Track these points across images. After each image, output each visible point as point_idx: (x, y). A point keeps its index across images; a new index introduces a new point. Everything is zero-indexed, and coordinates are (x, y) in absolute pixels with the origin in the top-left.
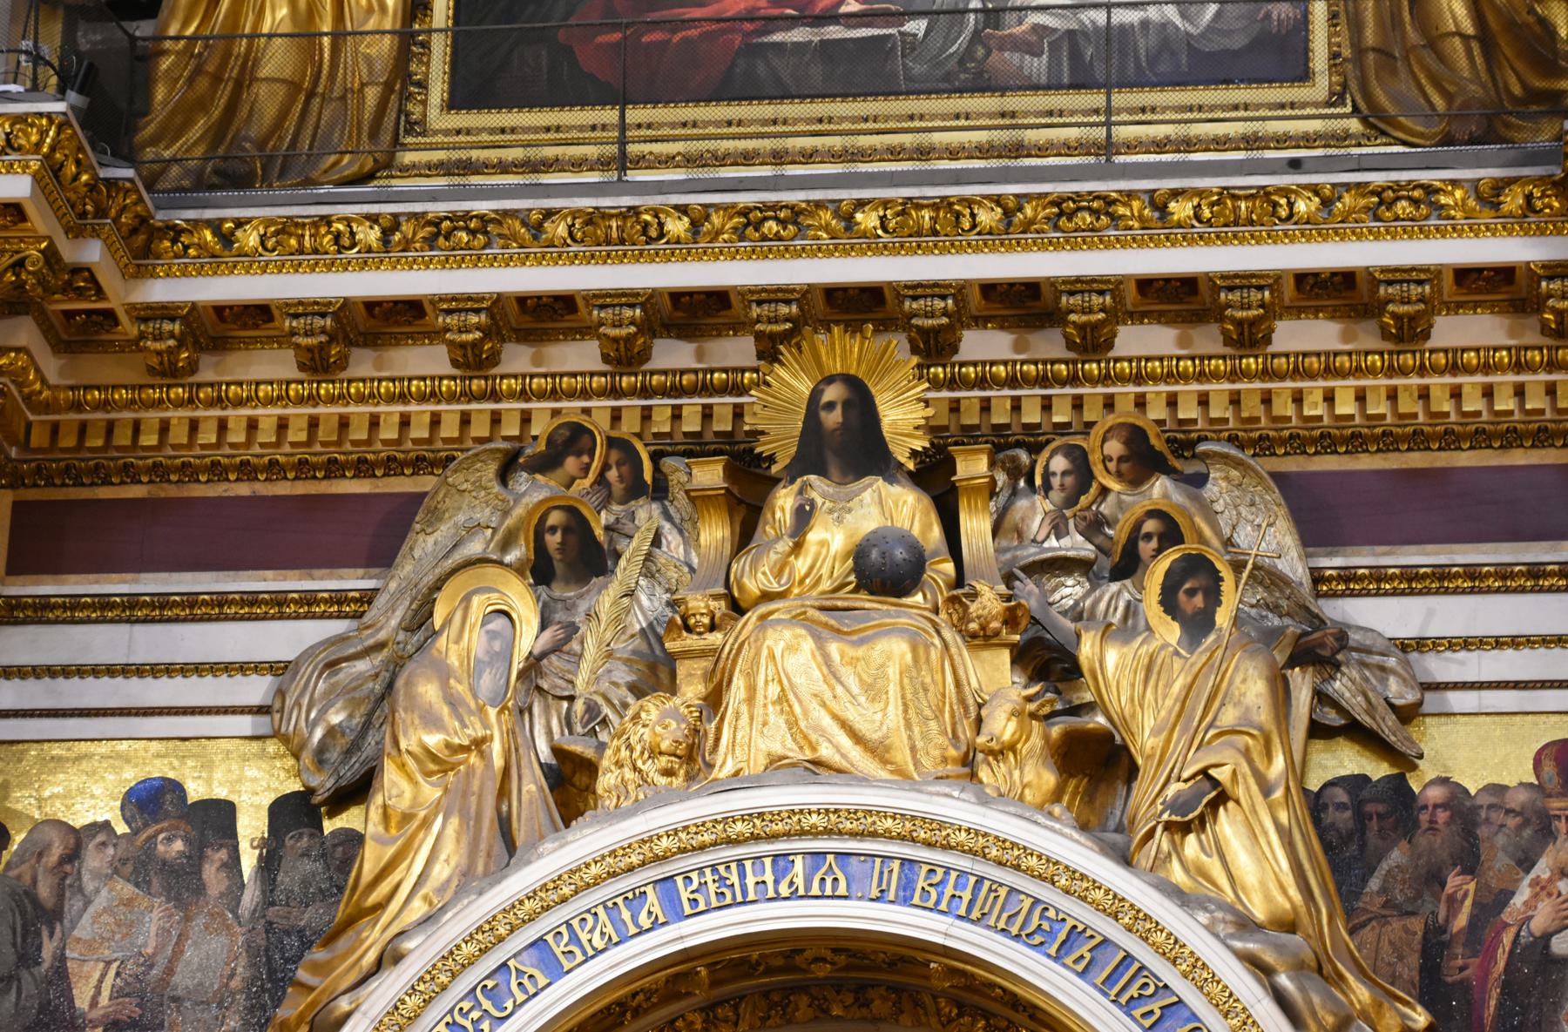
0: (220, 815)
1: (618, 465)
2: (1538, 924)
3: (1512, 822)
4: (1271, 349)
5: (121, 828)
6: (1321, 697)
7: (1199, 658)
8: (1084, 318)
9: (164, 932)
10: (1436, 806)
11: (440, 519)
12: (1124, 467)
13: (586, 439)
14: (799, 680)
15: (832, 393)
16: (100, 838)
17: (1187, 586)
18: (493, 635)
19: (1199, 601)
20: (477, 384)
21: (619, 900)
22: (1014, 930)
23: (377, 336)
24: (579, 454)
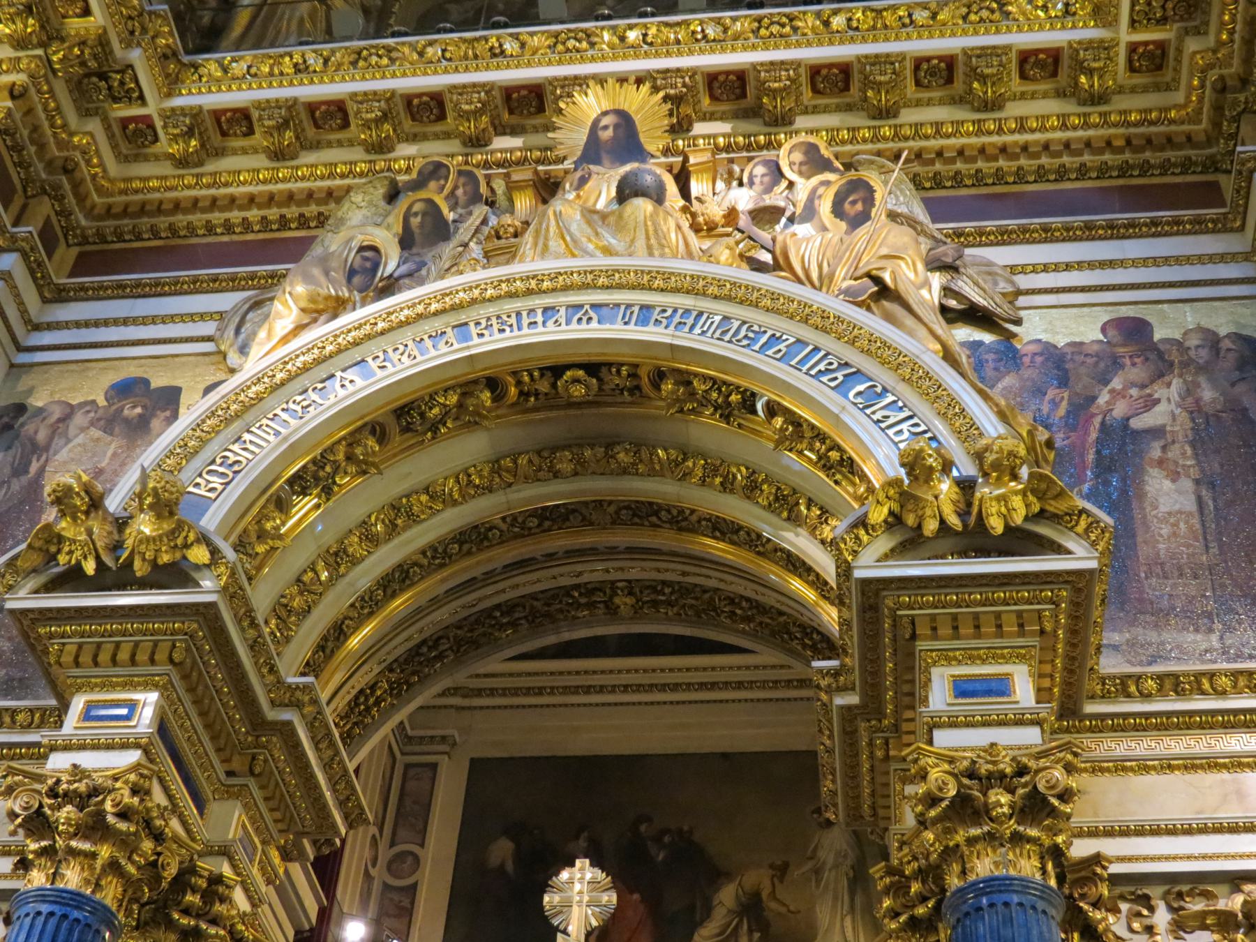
1: (464, 185)
2: (1120, 410)
3: (1089, 360)
6: (947, 291)
7: (864, 231)
8: (776, 85)
9: (115, 455)
11: (343, 224)
12: (804, 168)
13: (443, 171)
14: (574, 228)
15: (606, 121)
16: (88, 408)
17: (851, 199)
18: (366, 259)
20: (381, 165)
21: (426, 337)
22: (727, 338)
23: (319, 142)
24: (438, 179)
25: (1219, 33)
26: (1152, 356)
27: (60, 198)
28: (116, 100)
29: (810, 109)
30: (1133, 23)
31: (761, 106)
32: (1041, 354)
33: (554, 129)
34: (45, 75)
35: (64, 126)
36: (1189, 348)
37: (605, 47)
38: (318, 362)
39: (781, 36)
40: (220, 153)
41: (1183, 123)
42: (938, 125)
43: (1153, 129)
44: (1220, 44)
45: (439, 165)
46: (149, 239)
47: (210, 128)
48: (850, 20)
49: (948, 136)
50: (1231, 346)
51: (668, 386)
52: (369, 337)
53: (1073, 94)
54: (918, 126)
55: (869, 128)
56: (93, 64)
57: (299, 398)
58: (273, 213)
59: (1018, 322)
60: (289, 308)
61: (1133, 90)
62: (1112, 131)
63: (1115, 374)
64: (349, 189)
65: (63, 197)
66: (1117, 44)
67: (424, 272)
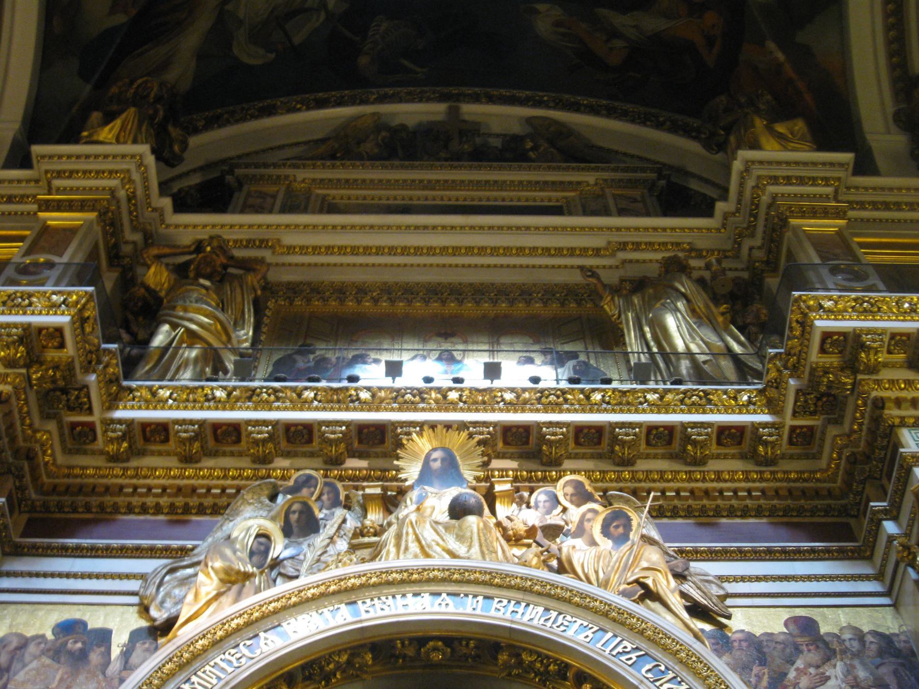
0: (104, 636)
1: (328, 493)
3: (779, 647)
4: (635, 468)
5: (50, 636)
7: (625, 547)
10: (740, 641)
11: (237, 515)
12: (574, 498)
13: (313, 482)
15: (437, 455)
16: (40, 640)
17: (614, 524)
18: (260, 544)
19: (621, 530)
24: (309, 487)
25: (852, 424)
26: (821, 645)
27: (20, 477)
28: (71, 408)
29: (572, 456)
30: (795, 414)
31: (540, 450)
32: (746, 640)
33: (398, 458)
34: (24, 388)
35: (31, 426)
36: (844, 640)
37: (432, 402)
38: (248, 624)
39: (557, 404)
40: (142, 453)
41: (825, 482)
42: (662, 473)
43: (805, 485)
44: (853, 432)
45: (309, 478)
46: (83, 512)
47: (137, 437)
48: (603, 396)
49: (668, 481)
50: (873, 640)
51: (503, 657)
52: (285, 608)
53: (752, 457)
54: (649, 472)
55: (614, 472)
56: (61, 383)
57: (233, 651)
58: (180, 501)
59: (729, 617)
60: (211, 578)
61: (791, 457)
62: (778, 484)
63: (798, 657)
64: (238, 491)
65: (23, 476)
66: (784, 427)
67: (301, 557)
